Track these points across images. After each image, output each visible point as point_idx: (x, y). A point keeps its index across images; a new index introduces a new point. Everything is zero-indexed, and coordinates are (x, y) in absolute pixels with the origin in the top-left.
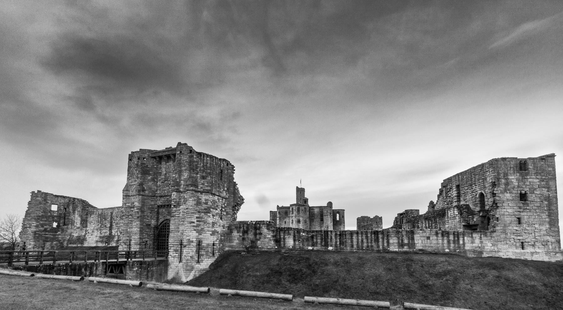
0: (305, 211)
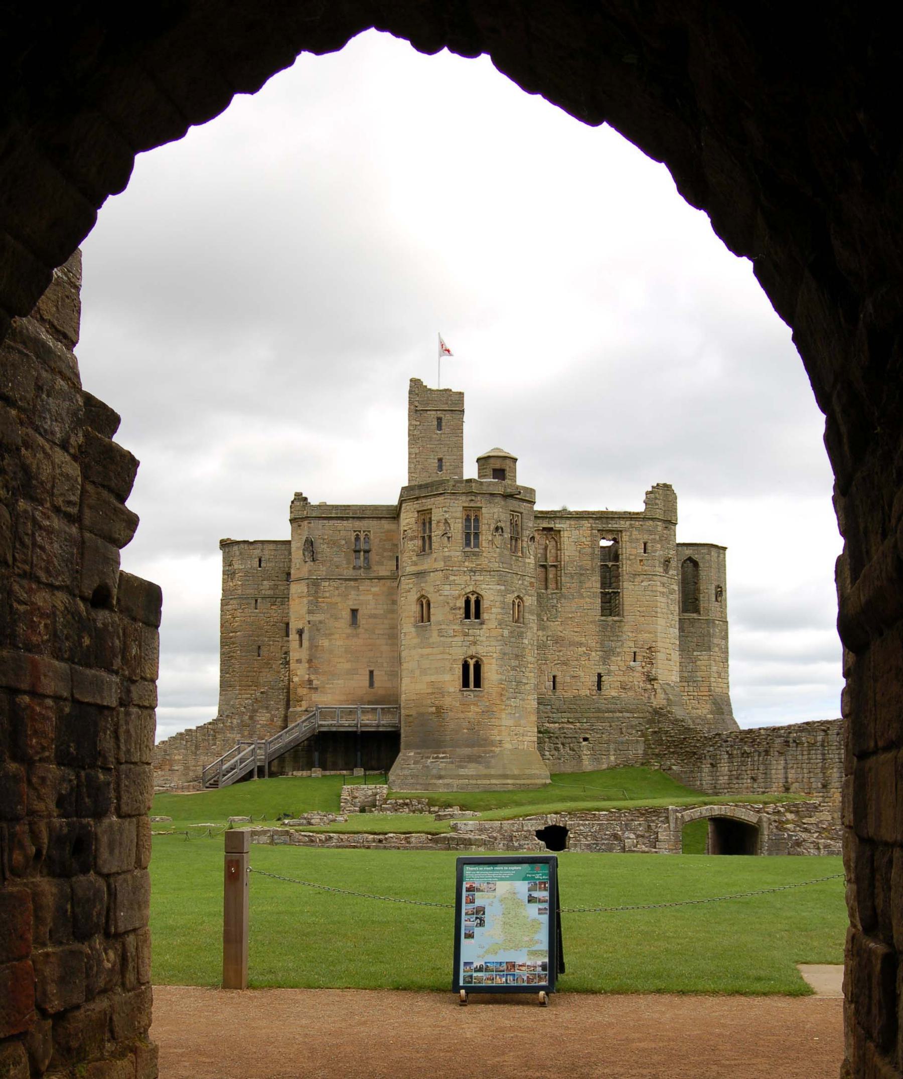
0: (515, 539)
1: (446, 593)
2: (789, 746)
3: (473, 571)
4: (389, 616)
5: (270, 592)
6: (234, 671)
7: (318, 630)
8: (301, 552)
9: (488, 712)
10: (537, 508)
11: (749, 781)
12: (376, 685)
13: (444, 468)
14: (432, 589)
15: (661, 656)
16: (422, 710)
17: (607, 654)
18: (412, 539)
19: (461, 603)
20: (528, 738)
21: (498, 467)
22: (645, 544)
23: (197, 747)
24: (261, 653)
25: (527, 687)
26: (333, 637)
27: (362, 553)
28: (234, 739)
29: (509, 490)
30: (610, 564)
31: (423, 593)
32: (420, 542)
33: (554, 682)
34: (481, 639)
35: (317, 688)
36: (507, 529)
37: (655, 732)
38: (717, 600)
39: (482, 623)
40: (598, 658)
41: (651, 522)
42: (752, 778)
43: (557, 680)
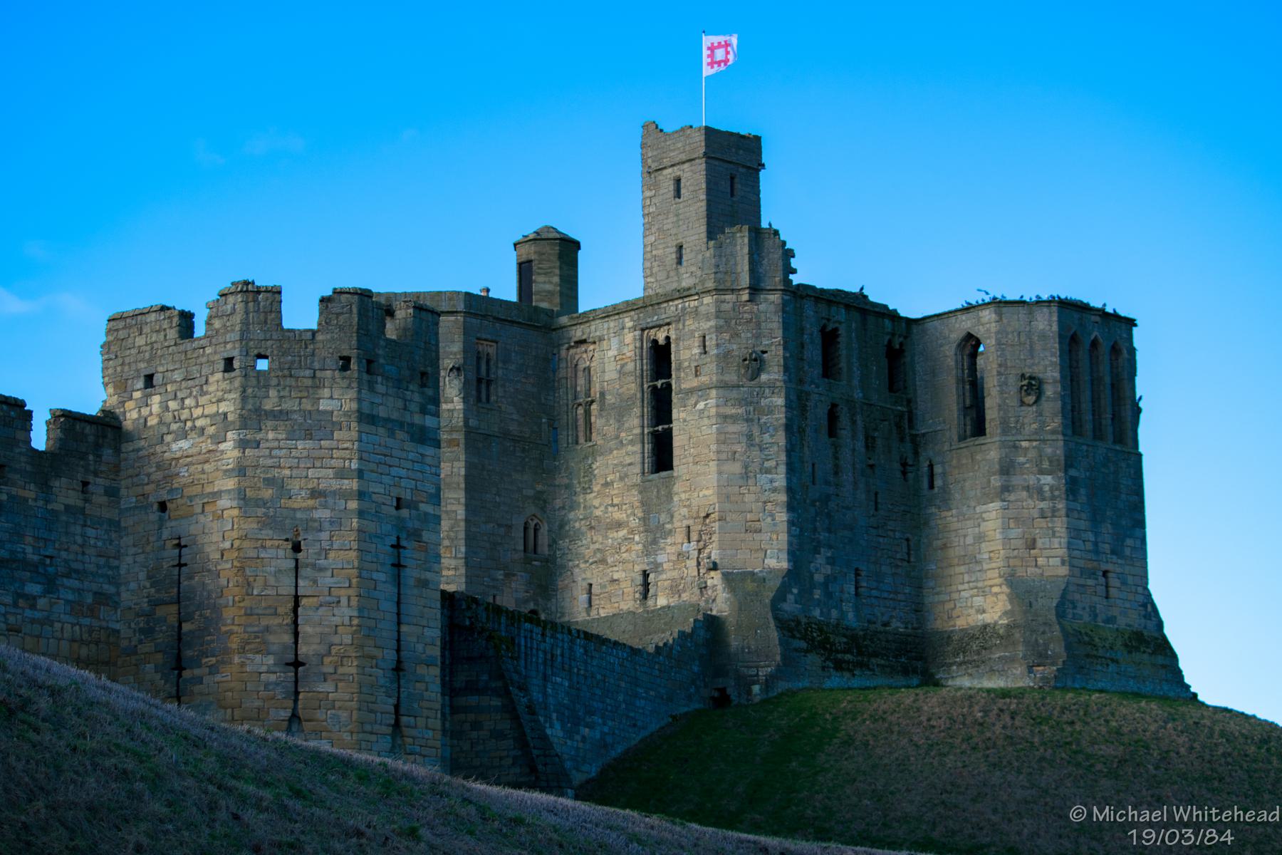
43: (595, 590)
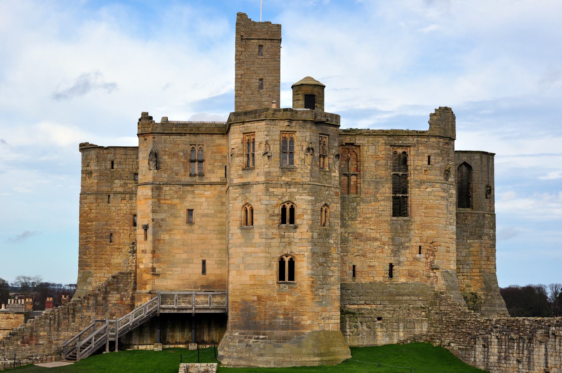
1: (266, 202)
2: (549, 337)
3: (288, 184)
4: (219, 215)
5: (121, 190)
6: (90, 254)
7: (160, 226)
8: (147, 161)
9: (300, 302)
10: (340, 128)
11: (515, 362)
12: (208, 271)
13: (264, 87)
14: (254, 199)
15: (441, 249)
16: (247, 298)
17: (398, 248)
18: (238, 156)
19: (278, 211)
20: (332, 321)
21: (311, 94)
22: (429, 157)
23: (59, 325)
24: (113, 239)
25: (332, 279)
26: (173, 232)
27: (197, 163)
28: (89, 317)
29: (319, 118)
30: (400, 173)
31: (248, 201)
32: (245, 159)
33: (354, 271)
34: (295, 240)
35: (158, 275)
36: (317, 150)
37: (437, 313)
38: (487, 198)
39: (296, 227)
40: (389, 251)
41: (433, 139)
42: (519, 362)
43: (357, 269)
